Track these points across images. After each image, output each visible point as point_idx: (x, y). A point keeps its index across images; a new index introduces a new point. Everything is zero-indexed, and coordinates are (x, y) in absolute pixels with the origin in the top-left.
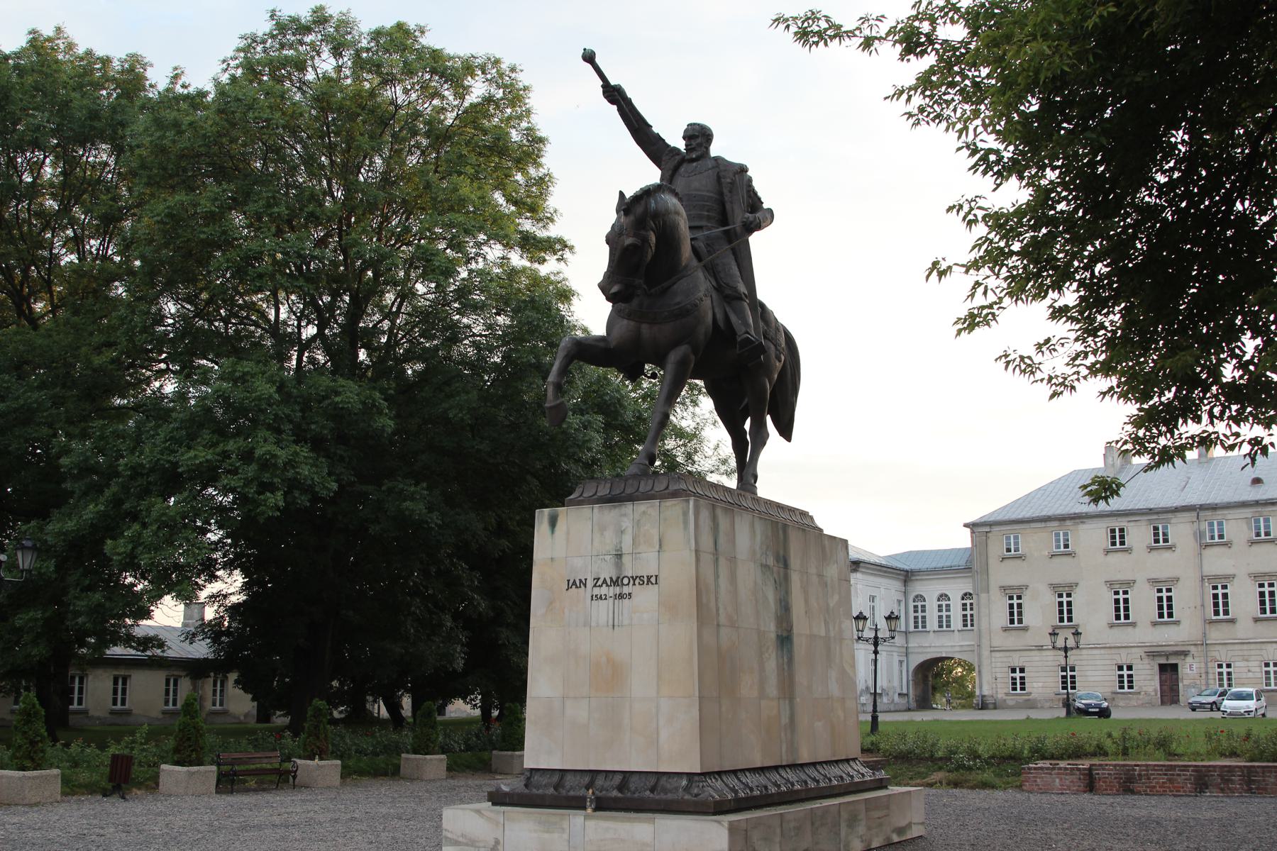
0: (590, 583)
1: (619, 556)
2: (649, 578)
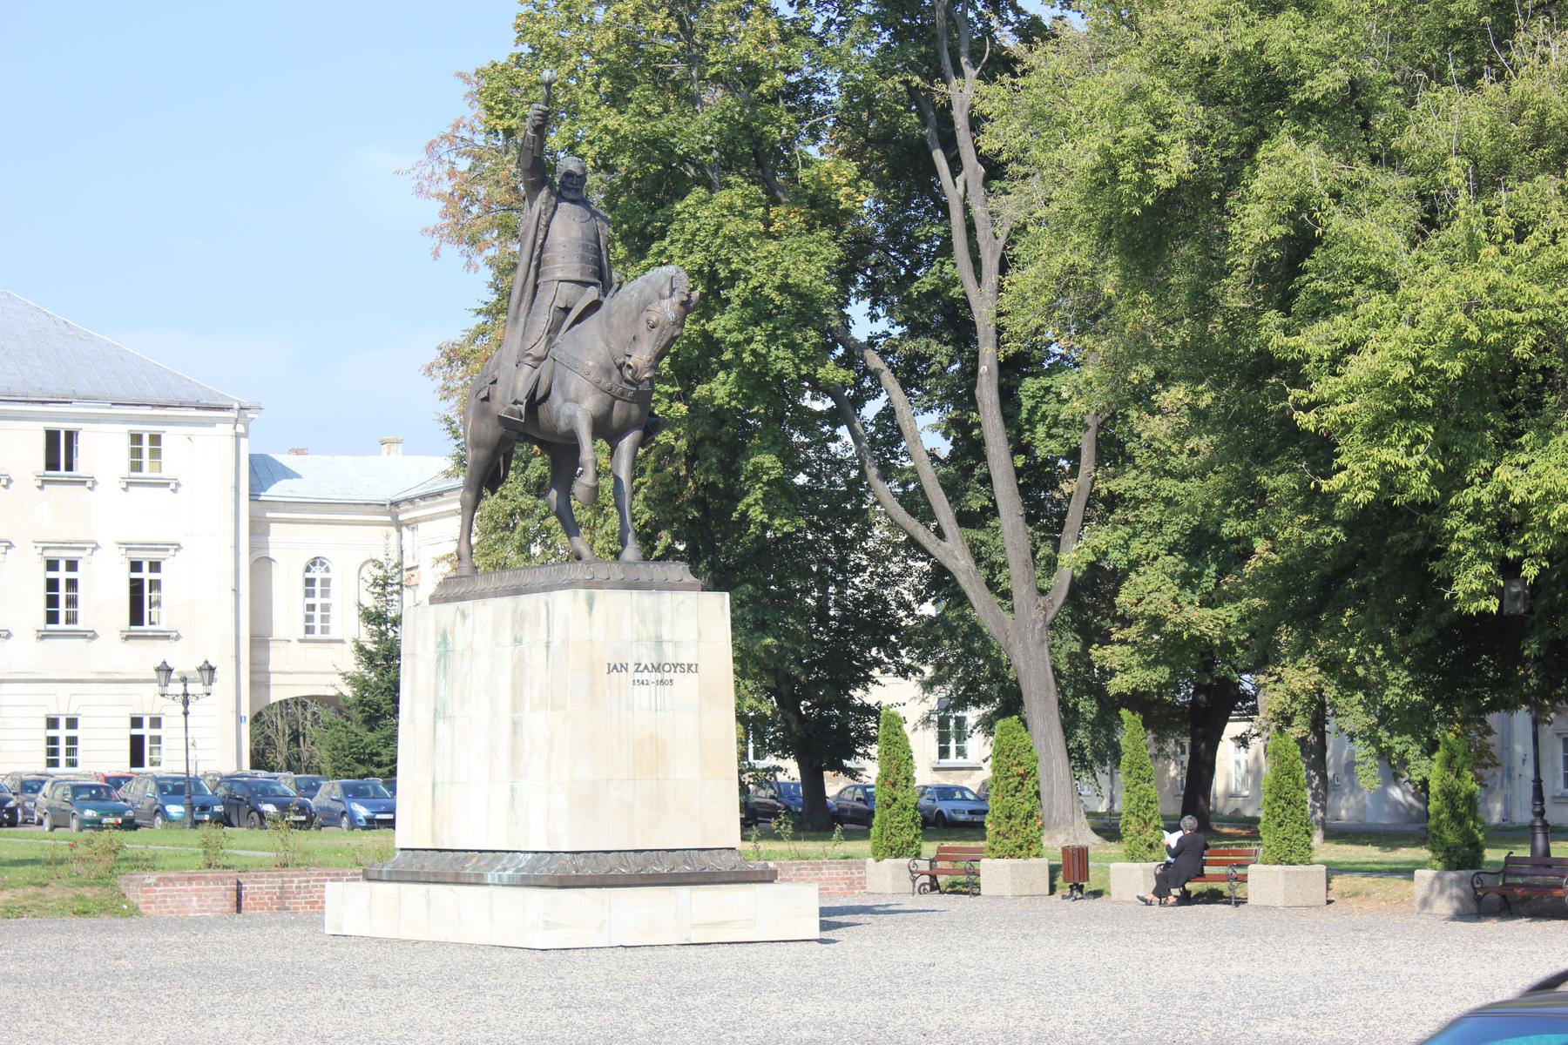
0: (632, 668)
1: (659, 642)
2: (690, 666)
